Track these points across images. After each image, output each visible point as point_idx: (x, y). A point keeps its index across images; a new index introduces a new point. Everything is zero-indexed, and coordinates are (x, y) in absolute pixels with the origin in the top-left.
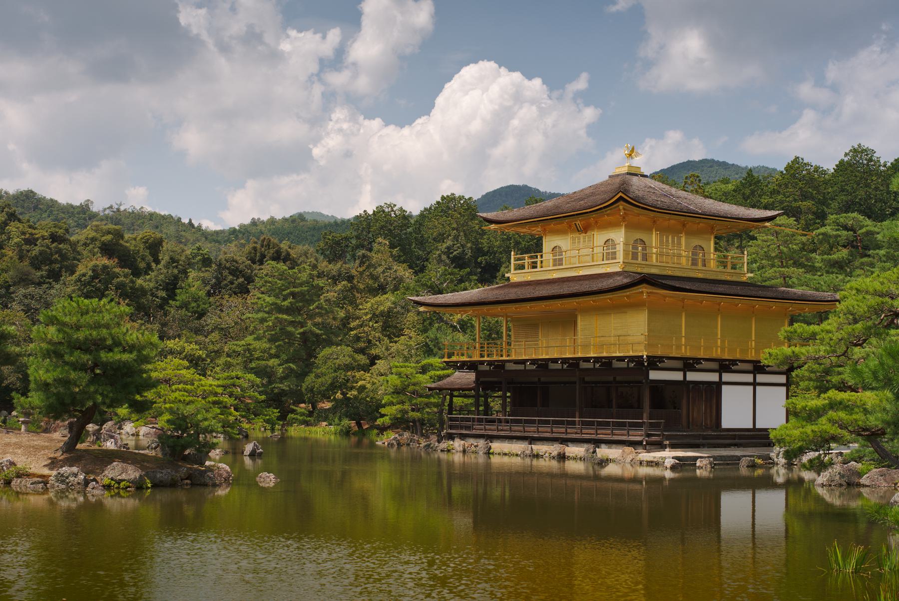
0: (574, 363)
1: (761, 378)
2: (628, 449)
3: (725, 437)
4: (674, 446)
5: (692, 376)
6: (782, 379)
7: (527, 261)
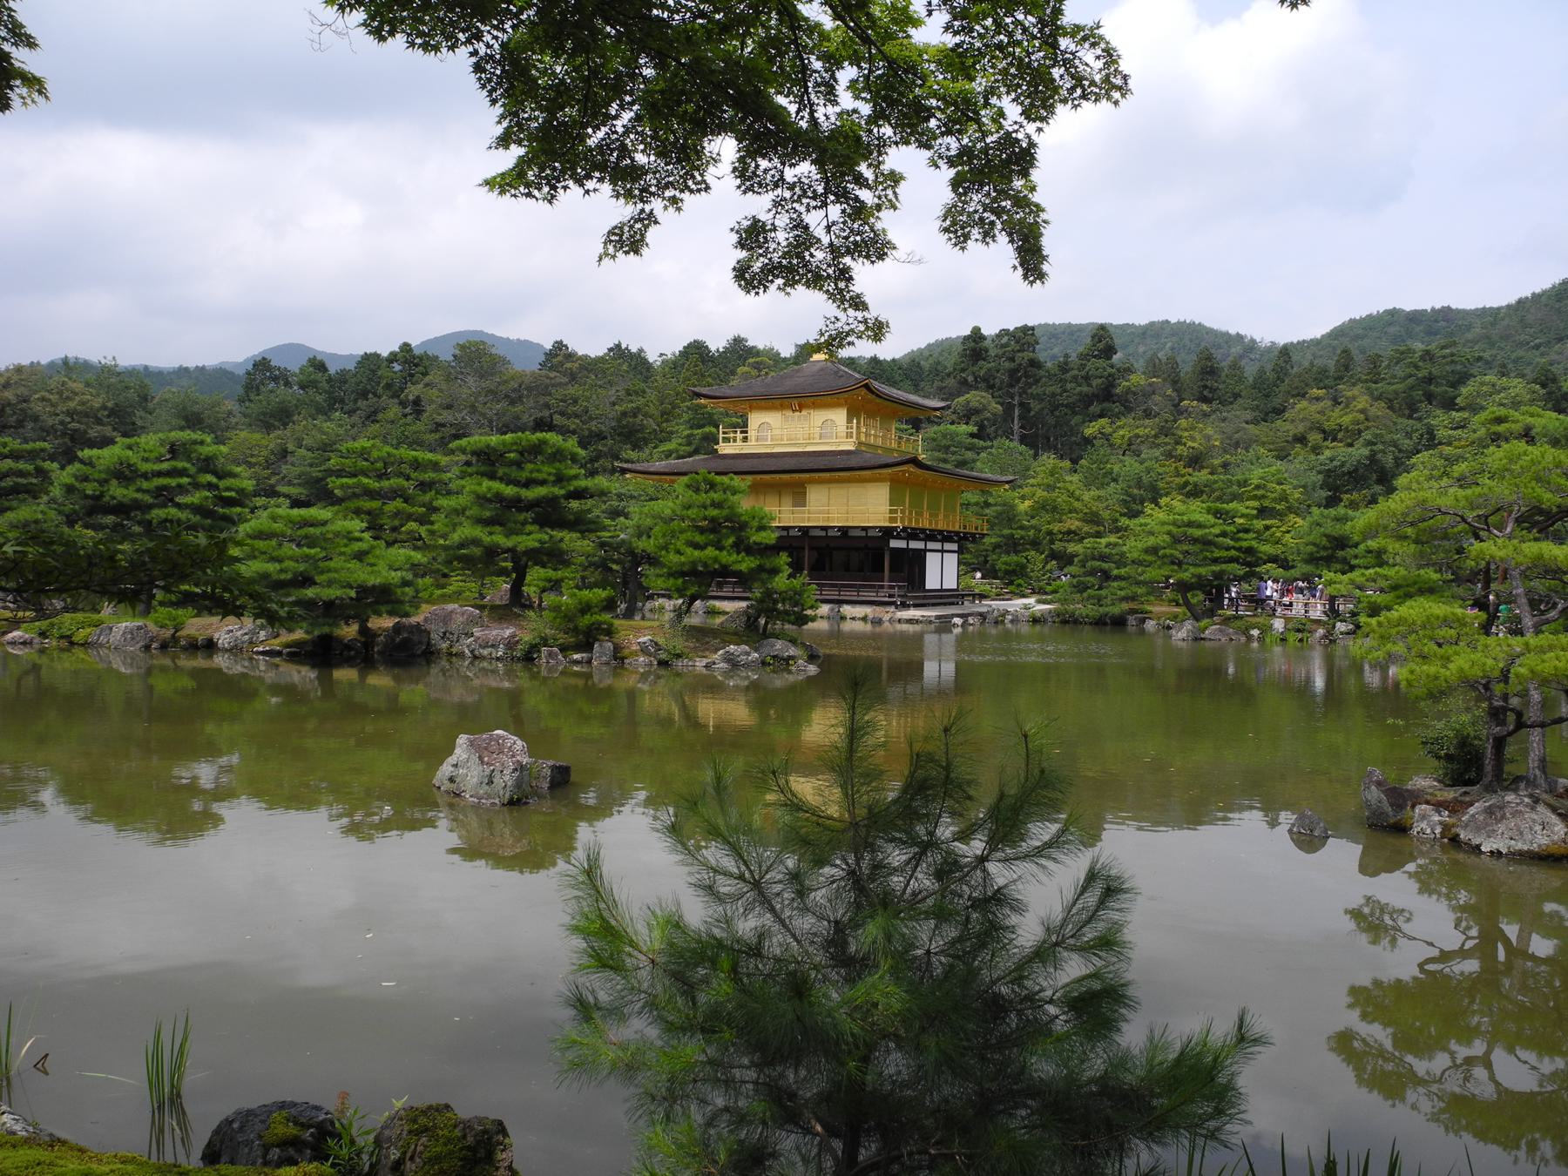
0: (805, 530)
1: (948, 546)
2: (878, 609)
3: (925, 597)
4: (916, 606)
5: (915, 545)
6: (954, 547)
7: (739, 436)
